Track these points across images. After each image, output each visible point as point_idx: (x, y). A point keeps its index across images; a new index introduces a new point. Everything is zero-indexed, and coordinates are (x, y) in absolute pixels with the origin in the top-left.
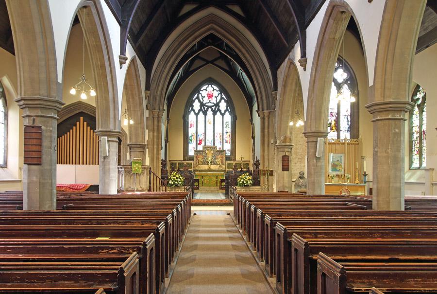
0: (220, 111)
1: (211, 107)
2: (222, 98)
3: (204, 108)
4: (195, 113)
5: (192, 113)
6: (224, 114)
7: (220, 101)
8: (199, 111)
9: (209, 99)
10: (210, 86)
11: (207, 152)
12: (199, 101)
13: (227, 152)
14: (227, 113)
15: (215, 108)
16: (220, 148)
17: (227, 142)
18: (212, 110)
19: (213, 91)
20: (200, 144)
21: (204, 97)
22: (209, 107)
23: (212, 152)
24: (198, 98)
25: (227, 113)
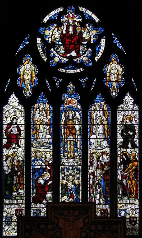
0: (105, 92)
1: (74, 78)
2: (110, 49)
3: (53, 83)
4: (22, 100)
5: (13, 99)
6: (120, 100)
7: (105, 60)
8: (37, 91)
9: (68, 51)
10: (71, 12)
11: (62, 223)
12: (37, 61)
13: (128, 225)
14: (128, 99)
15: (89, 83)
16: (104, 212)
17: (126, 193)
18: (79, 89)
19: (82, 25)
20: (38, 200)
21: (53, 45)
22: (68, 78)
23: (80, 223)
24: (32, 49)
25: (128, 99)
